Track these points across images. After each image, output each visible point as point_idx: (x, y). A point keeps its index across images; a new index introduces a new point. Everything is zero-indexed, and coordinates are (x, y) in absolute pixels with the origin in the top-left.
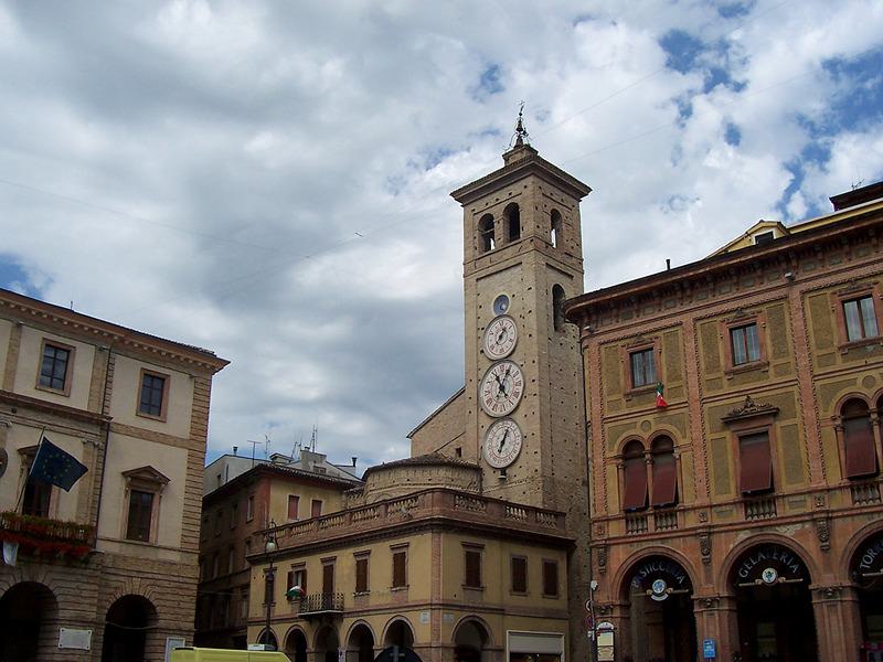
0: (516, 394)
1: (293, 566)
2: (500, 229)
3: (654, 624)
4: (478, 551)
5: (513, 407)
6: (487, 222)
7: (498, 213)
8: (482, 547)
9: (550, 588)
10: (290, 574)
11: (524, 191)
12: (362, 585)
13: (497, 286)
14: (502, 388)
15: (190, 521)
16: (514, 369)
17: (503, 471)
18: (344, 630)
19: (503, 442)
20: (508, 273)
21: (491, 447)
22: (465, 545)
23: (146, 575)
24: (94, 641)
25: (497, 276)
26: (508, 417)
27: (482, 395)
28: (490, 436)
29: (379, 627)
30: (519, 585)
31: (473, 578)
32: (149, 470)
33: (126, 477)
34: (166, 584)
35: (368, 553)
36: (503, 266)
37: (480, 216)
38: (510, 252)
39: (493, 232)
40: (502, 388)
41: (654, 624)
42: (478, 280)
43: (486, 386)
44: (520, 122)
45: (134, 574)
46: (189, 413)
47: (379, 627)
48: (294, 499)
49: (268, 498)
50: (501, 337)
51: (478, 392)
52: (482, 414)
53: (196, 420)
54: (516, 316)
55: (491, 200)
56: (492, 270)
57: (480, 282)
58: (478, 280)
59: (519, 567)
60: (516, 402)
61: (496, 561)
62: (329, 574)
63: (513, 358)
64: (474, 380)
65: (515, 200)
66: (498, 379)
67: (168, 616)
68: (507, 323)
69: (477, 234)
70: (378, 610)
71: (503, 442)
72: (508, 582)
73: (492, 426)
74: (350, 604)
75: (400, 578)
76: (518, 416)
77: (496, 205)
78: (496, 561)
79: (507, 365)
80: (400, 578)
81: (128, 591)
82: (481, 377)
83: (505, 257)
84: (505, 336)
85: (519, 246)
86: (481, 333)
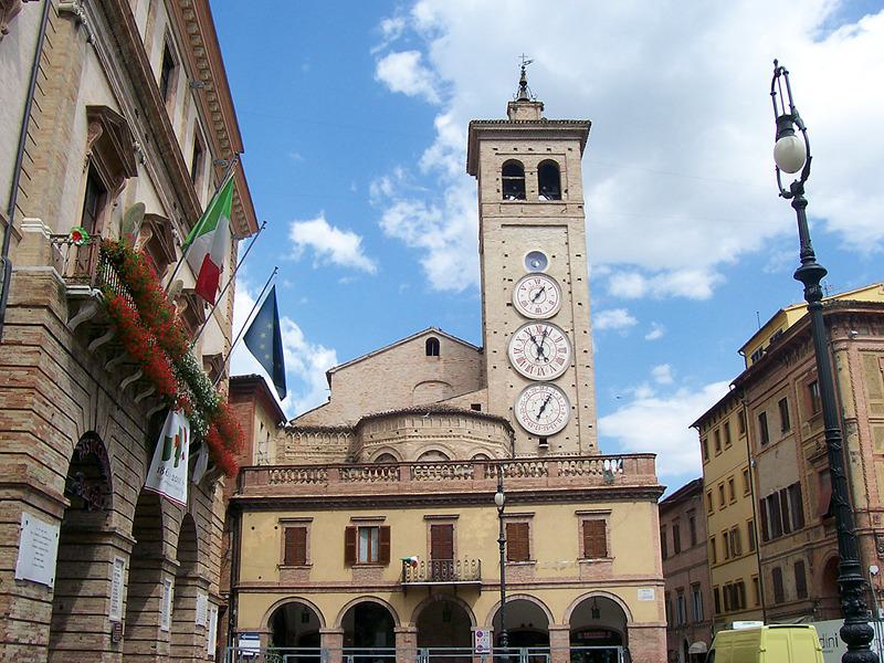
0: (561, 361)
1: (353, 520)
2: (532, 182)
3: (831, 609)
5: (555, 375)
6: (512, 169)
7: (531, 165)
10: (350, 534)
11: (568, 153)
14: (540, 351)
16: (555, 334)
17: (543, 440)
18: (483, 610)
19: (543, 409)
21: (524, 411)
25: (530, 230)
26: (550, 383)
27: (511, 352)
29: (560, 608)
35: (531, 516)
37: (505, 158)
40: (540, 351)
41: (831, 609)
43: (515, 344)
44: (523, 74)
47: (560, 608)
50: (538, 296)
51: (508, 344)
55: (523, 147)
56: (523, 221)
58: (503, 225)
62: (442, 542)
65: (554, 158)
66: (533, 339)
68: (545, 282)
70: (554, 584)
71: (543, 409)
73: (527, 388)
74: (491, 573)
76: (564, 384)
77: (531, 155)
79: (544, 327)
84: (542, 294)
85: (564, 207)
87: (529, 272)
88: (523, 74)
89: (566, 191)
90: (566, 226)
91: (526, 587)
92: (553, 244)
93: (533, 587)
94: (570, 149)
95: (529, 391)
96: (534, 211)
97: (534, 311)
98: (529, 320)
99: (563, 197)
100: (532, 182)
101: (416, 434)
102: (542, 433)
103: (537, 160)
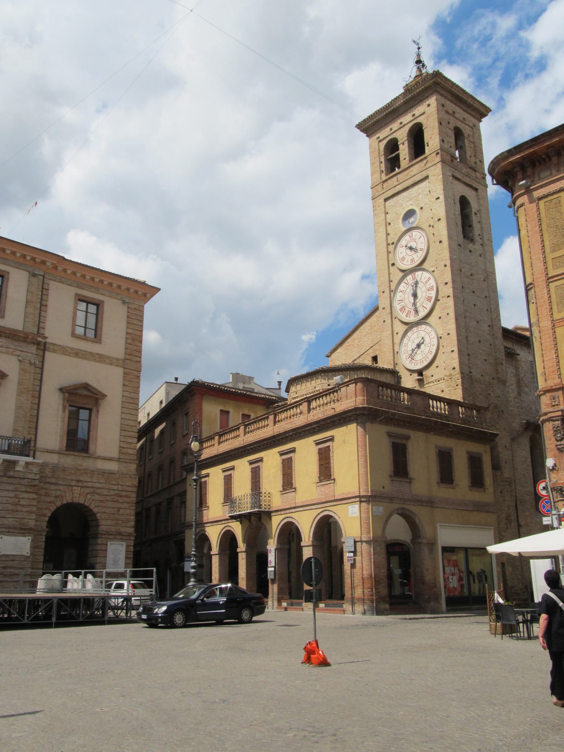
2: (404, 151)
4: (404, 442)
5: (426, 311)
7: (402, 135)
8: (408, 438)
9: (477, 481)
12: (288, 484)
13: (404, 203)
15: (127, 433)
16: (426, 275)
17: (420, 372)
20: (416, 188)
22: (390, 435)
23: (85, 484)
24: (34, 547)
25: (404, 194)
28: (405, 341)
30: (446, 476)
31: (400, 468)
32: (86, 386)
33: (63, 393)
34: (105, 492)
36: (410, 182)
37: (385, 142)
38: (415, 169)
39: (398, 155)
42: (386, 200)
43: (399, 296)
45: (73, 483)
46: (124, 336)
48: (225, 413)
49: (201, 409)
50: (411, 248)
52: (396, 322)
53: (129, 341)
54: (425, 226)
57: (388, 203)
59: (445, 459)
60: (429, 306)
61: (422, 452)
63: (425, 266)
64: (387, 292)
67: (109, 522)
69: (382, 159)
72: (435, 474)
75: (325, 472)
77: (400, 130)
78: (422, 452)
80: (325, 472)
81: (68, 499)
82: (393, 288)
83: (412, 174)
85: (425, 161)
86: (391, 248)
87: (404, 229)
88: (419, 55)
89: (428, 146)
90: (427, 177)
91: (288, 511)
92: (420, 197)
93: (293, 510)
94: (429, 105)
95: (409, 334)
96: (407, 175)
97: (409, 263)
98: (405, 273)
99: (426, 151)
100: (404, 151)
101: (297, 395)
102: (419, 367)
103: (406, 129)
